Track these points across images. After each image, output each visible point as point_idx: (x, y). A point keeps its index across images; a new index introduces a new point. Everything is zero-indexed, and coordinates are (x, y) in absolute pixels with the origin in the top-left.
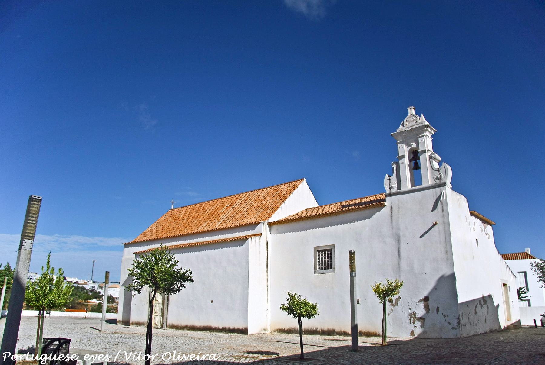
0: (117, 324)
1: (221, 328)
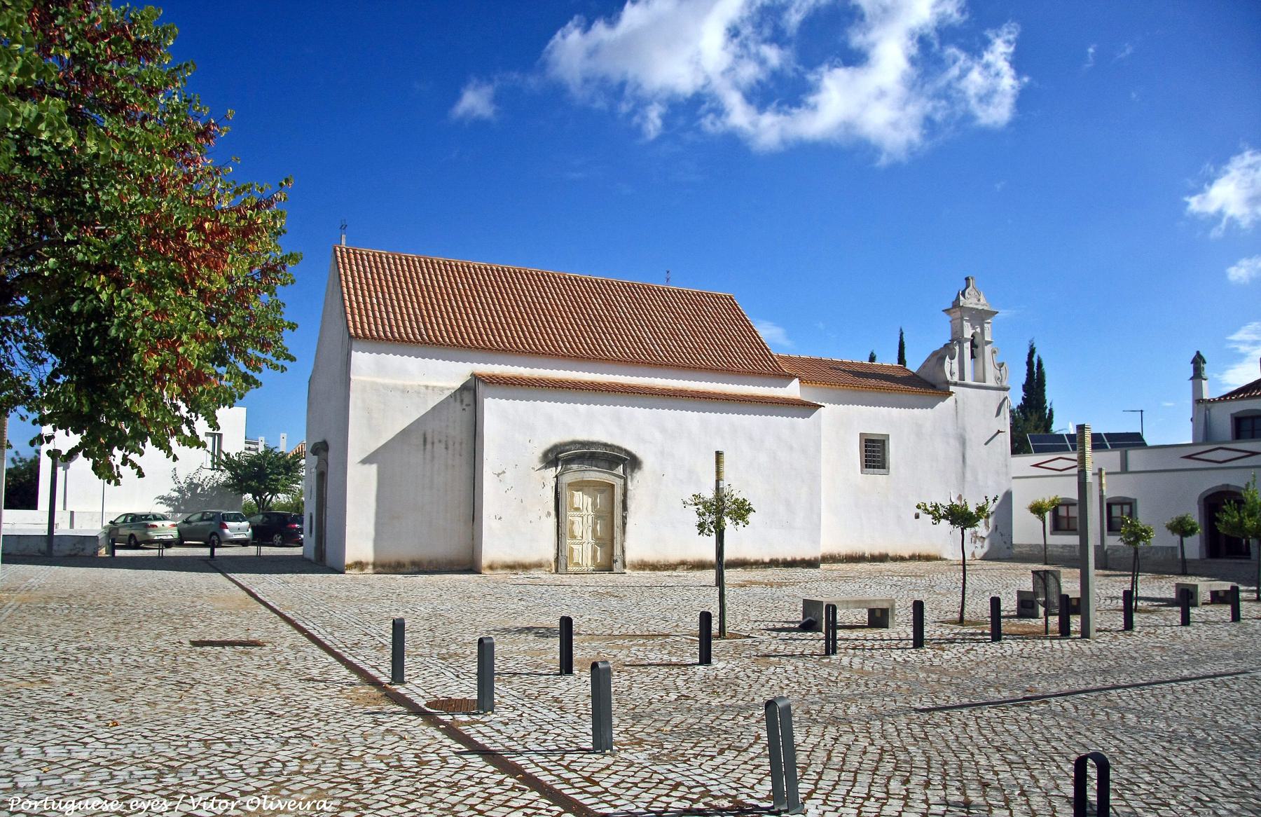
0: (347, 572)
1: (767, 559)
